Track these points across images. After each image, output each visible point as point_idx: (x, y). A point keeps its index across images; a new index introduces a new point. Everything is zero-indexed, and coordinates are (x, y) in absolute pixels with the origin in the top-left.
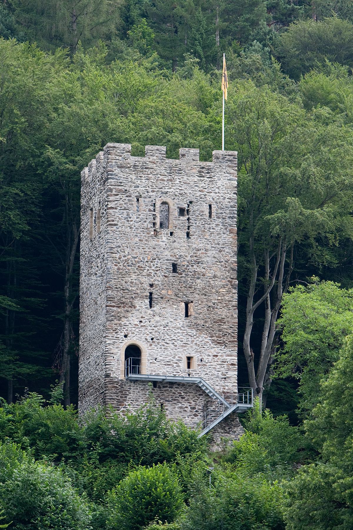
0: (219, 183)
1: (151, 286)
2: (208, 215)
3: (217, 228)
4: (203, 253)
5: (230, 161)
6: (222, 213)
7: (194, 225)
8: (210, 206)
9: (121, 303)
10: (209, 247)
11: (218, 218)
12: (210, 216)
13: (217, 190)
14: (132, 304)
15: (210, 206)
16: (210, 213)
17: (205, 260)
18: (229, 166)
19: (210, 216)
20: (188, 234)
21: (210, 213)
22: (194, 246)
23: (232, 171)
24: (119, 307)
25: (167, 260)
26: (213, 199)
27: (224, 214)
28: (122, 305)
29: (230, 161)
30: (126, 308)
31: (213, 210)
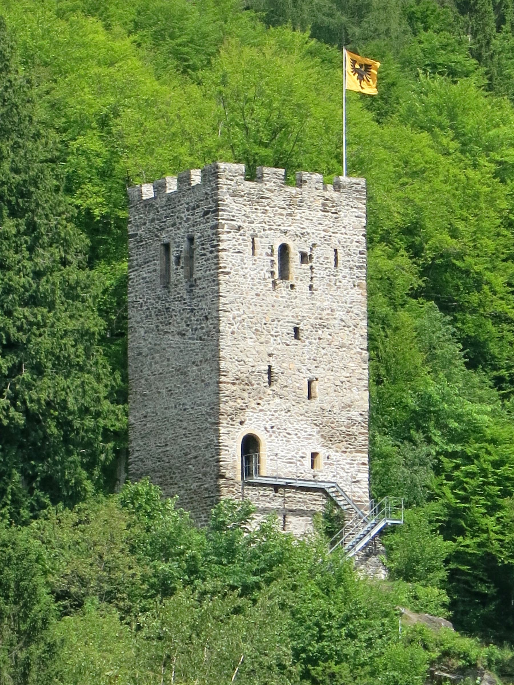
0: (346, 221)
1: (270, 355)
2: (333, 262)
3: (343, 281)
4: (328, 314)
5: (358, 191)
6: (349, 261)
7: (318, 276)
8: (336, 250)
9: (237, 379)
10: (335, 306)
11: (346, 267)
12: (336, 265)
13: (343, 230)
14: (249, 380)
15: (336, 250)
16: (336, 259)
17: (332, 322)
18: (357, 198)
19: (336, 265)
20: (311, 287)
21: (336, 259)
22: (318, 304)
23: (360, 205)
24: (234, 384)
25: (288, 322)
26: (339, 242)
27: (351, 262)
28: (237, 382)
29: (358, 191)
30: (242, 386)
31: (339, 256)
